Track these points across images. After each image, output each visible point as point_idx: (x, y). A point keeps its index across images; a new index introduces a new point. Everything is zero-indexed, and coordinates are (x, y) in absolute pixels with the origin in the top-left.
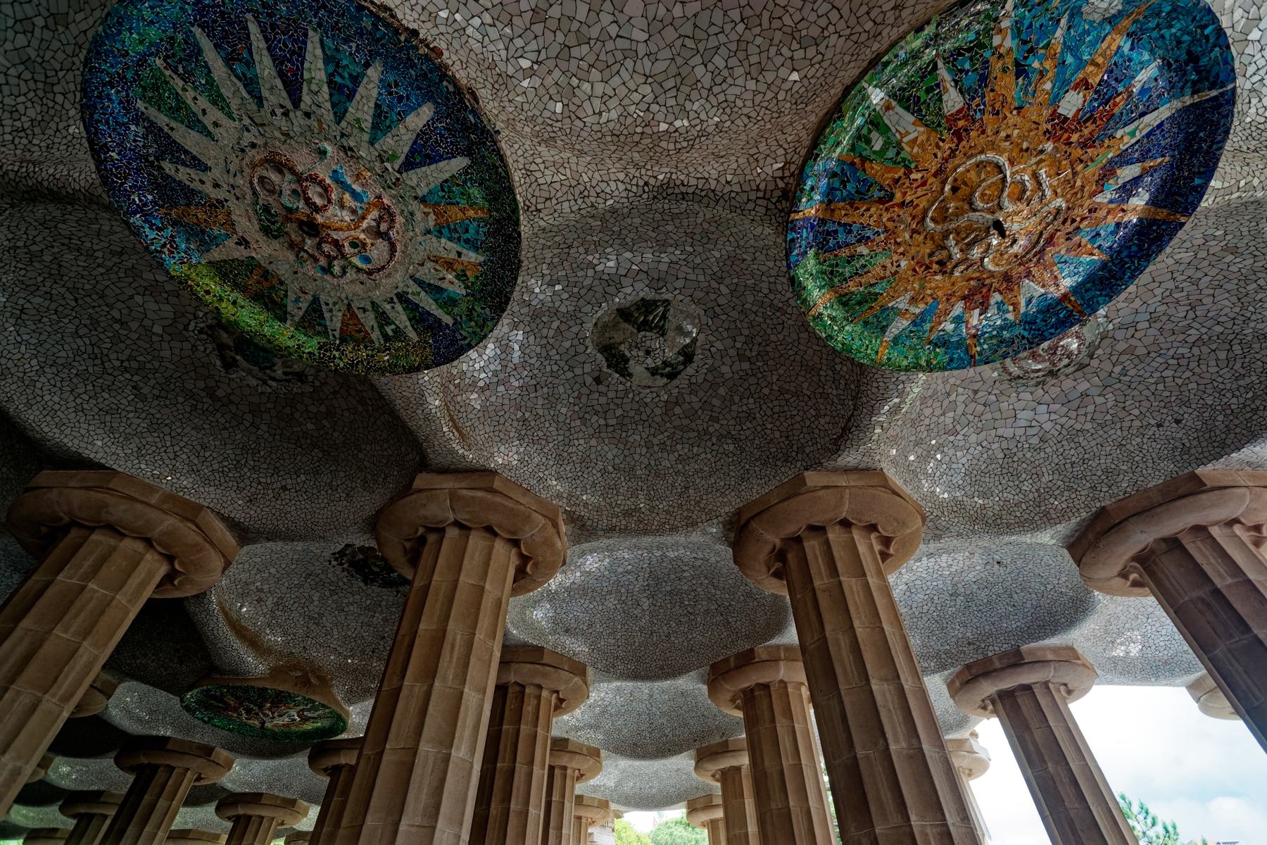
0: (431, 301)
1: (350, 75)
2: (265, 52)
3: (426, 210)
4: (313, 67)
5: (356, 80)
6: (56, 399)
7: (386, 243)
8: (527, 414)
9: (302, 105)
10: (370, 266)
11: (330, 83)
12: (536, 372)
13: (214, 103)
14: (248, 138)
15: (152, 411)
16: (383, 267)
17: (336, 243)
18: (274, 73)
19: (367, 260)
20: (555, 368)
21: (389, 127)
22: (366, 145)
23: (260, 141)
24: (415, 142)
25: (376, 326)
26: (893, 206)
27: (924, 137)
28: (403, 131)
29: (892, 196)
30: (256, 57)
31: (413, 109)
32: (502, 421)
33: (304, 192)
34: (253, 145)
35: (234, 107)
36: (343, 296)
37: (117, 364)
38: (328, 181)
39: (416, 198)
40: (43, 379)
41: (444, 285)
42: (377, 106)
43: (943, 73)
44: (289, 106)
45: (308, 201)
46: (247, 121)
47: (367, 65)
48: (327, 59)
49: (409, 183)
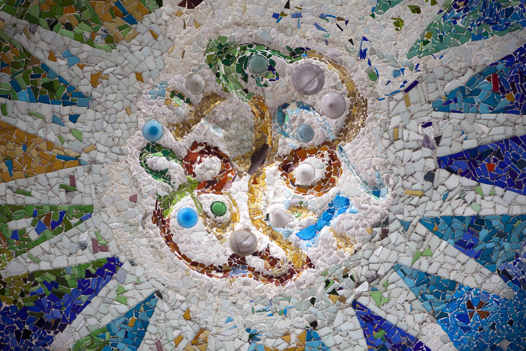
0: (106, 320)
1: (491, 251)
2: (509, 132)
3: (293, 338)
4: (497, 199)
5: (484, 258)
7: (224, 260)
9: (442, 173)
10: (173, 223)
11: (478, 222)
13: (430, 30)
14: (385, 72)
16: (175, 247)
18: (486, 140)
19: (187, 219)
21: (424, 299)
22: (394, 257)
23: (380, 87)
24: (403, 333)
25: (29, 200)
28: (419, 317)
30: (502, 117)
31: (451, 335)
33: (313, 152)
34: (374, 76)
35: (432, 62)
36: (100, 157)
38: (333, 191)
39: (314, 324)
42: (453, 284)
44: (443, 151)
45: (298, 155)
46: (410, 77)
47: (505, 275)
48: (509, 221)
49: (339, 317)
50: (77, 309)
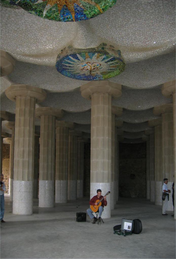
5: (68, 62)
6: (145, 82)
8: (171, 22)
11: (69, 64)
12: (156, 17)
15: (156, 71)
17: (94, 69)
20: (157, 11)
26: (67, 4)
27: (50, 4)
29: (65, 5)
32: (168, 31)
37: (142, 71)
40: (141, 81)
41: (103, 58)
43: (36, 3)
48: (66, 63)
50: (110, 60)
